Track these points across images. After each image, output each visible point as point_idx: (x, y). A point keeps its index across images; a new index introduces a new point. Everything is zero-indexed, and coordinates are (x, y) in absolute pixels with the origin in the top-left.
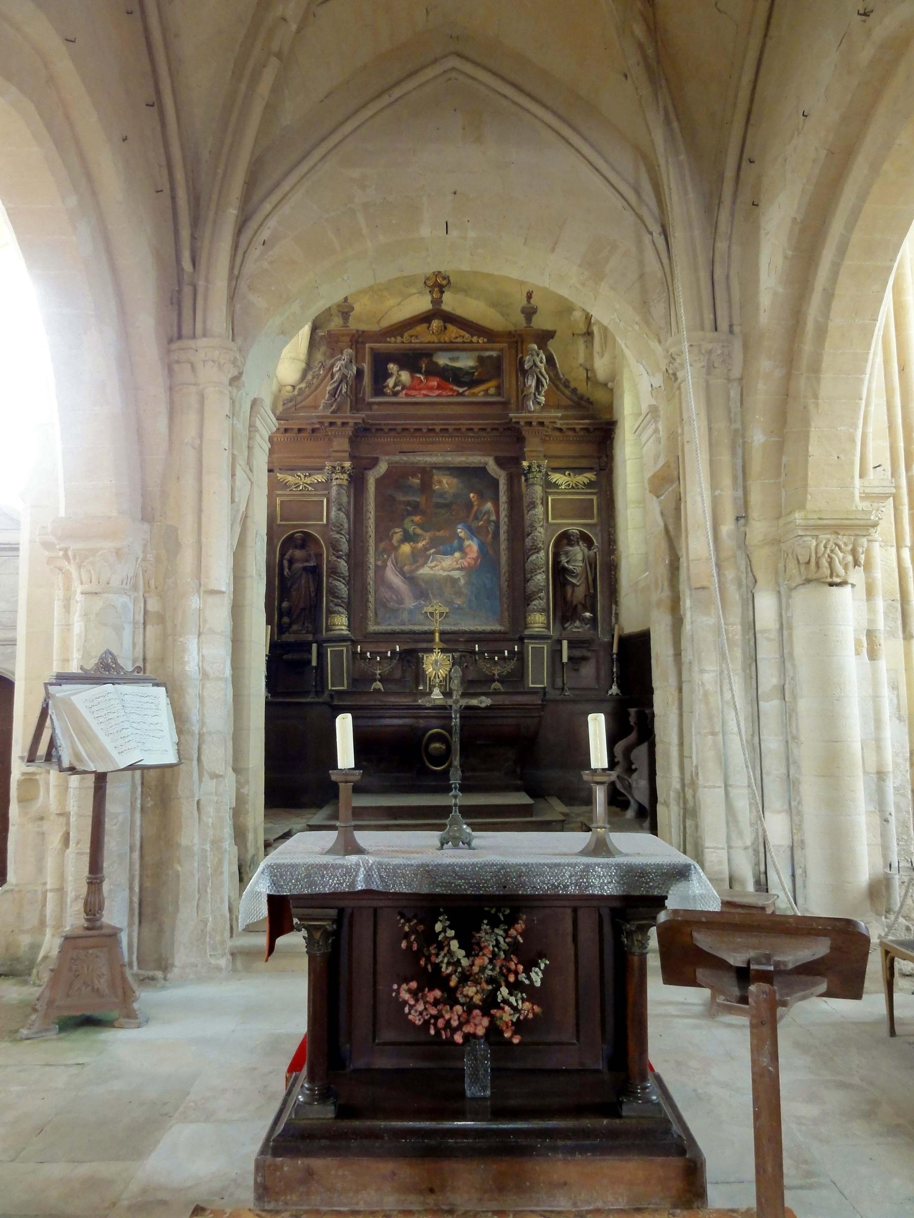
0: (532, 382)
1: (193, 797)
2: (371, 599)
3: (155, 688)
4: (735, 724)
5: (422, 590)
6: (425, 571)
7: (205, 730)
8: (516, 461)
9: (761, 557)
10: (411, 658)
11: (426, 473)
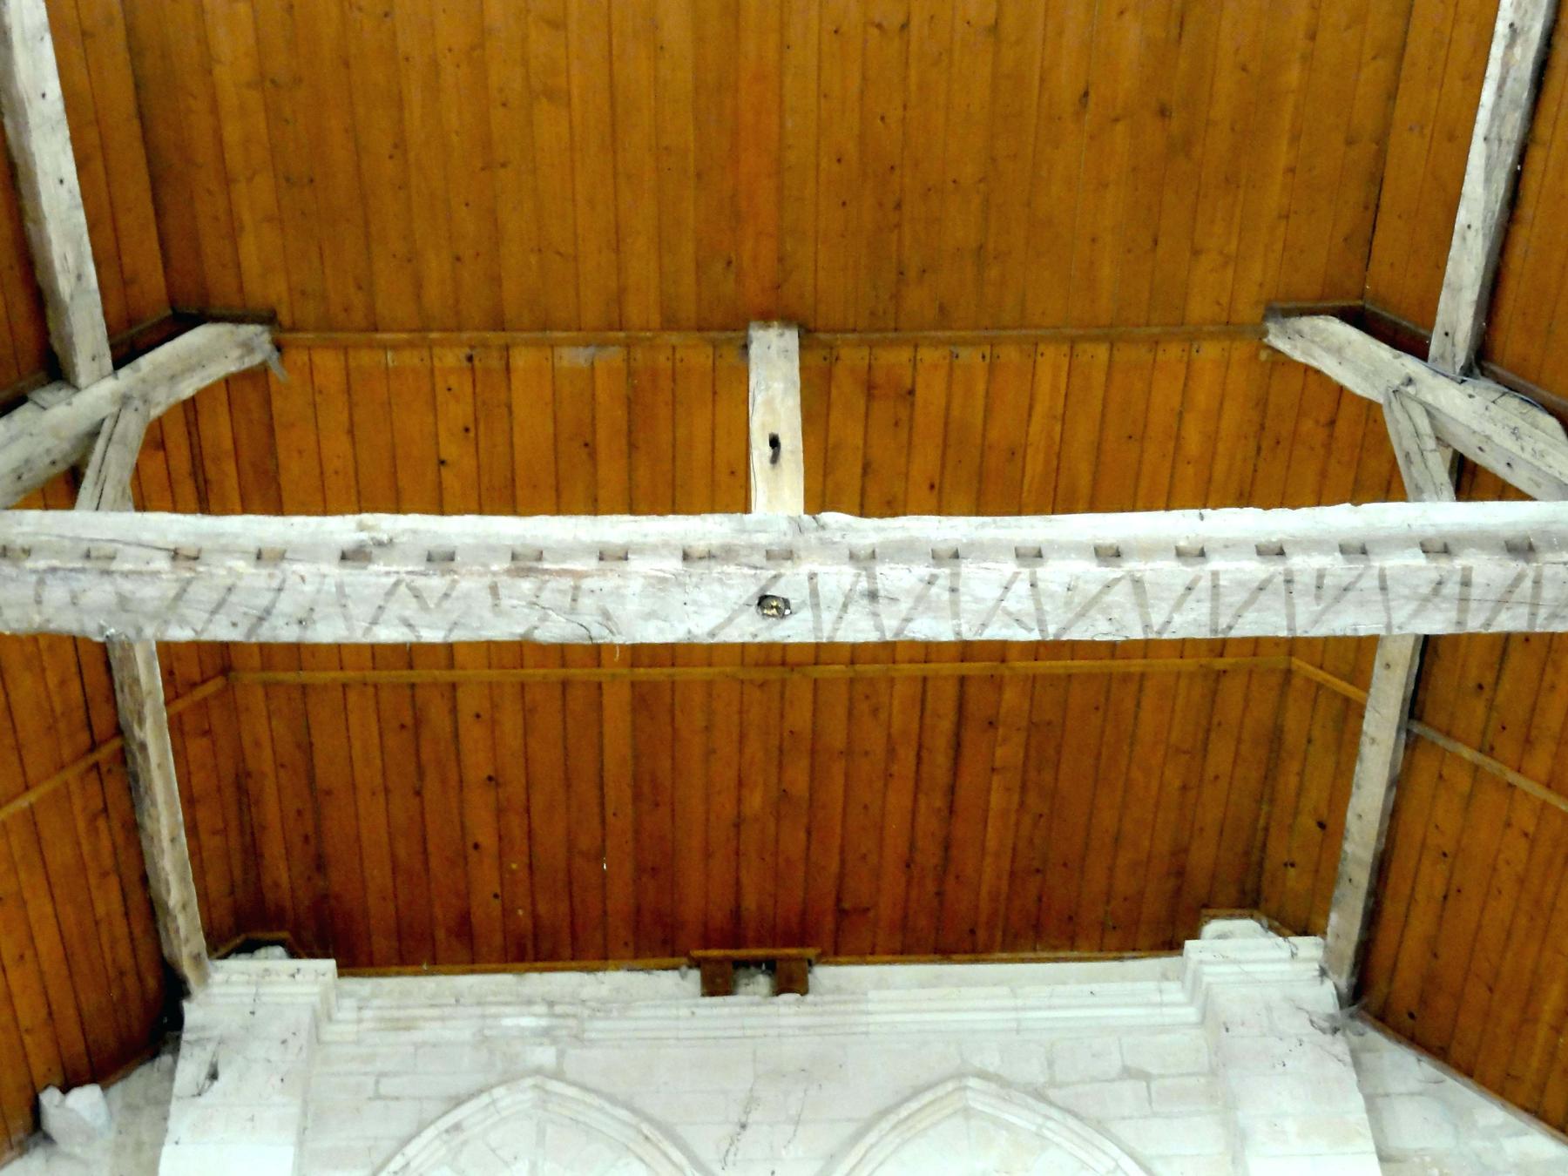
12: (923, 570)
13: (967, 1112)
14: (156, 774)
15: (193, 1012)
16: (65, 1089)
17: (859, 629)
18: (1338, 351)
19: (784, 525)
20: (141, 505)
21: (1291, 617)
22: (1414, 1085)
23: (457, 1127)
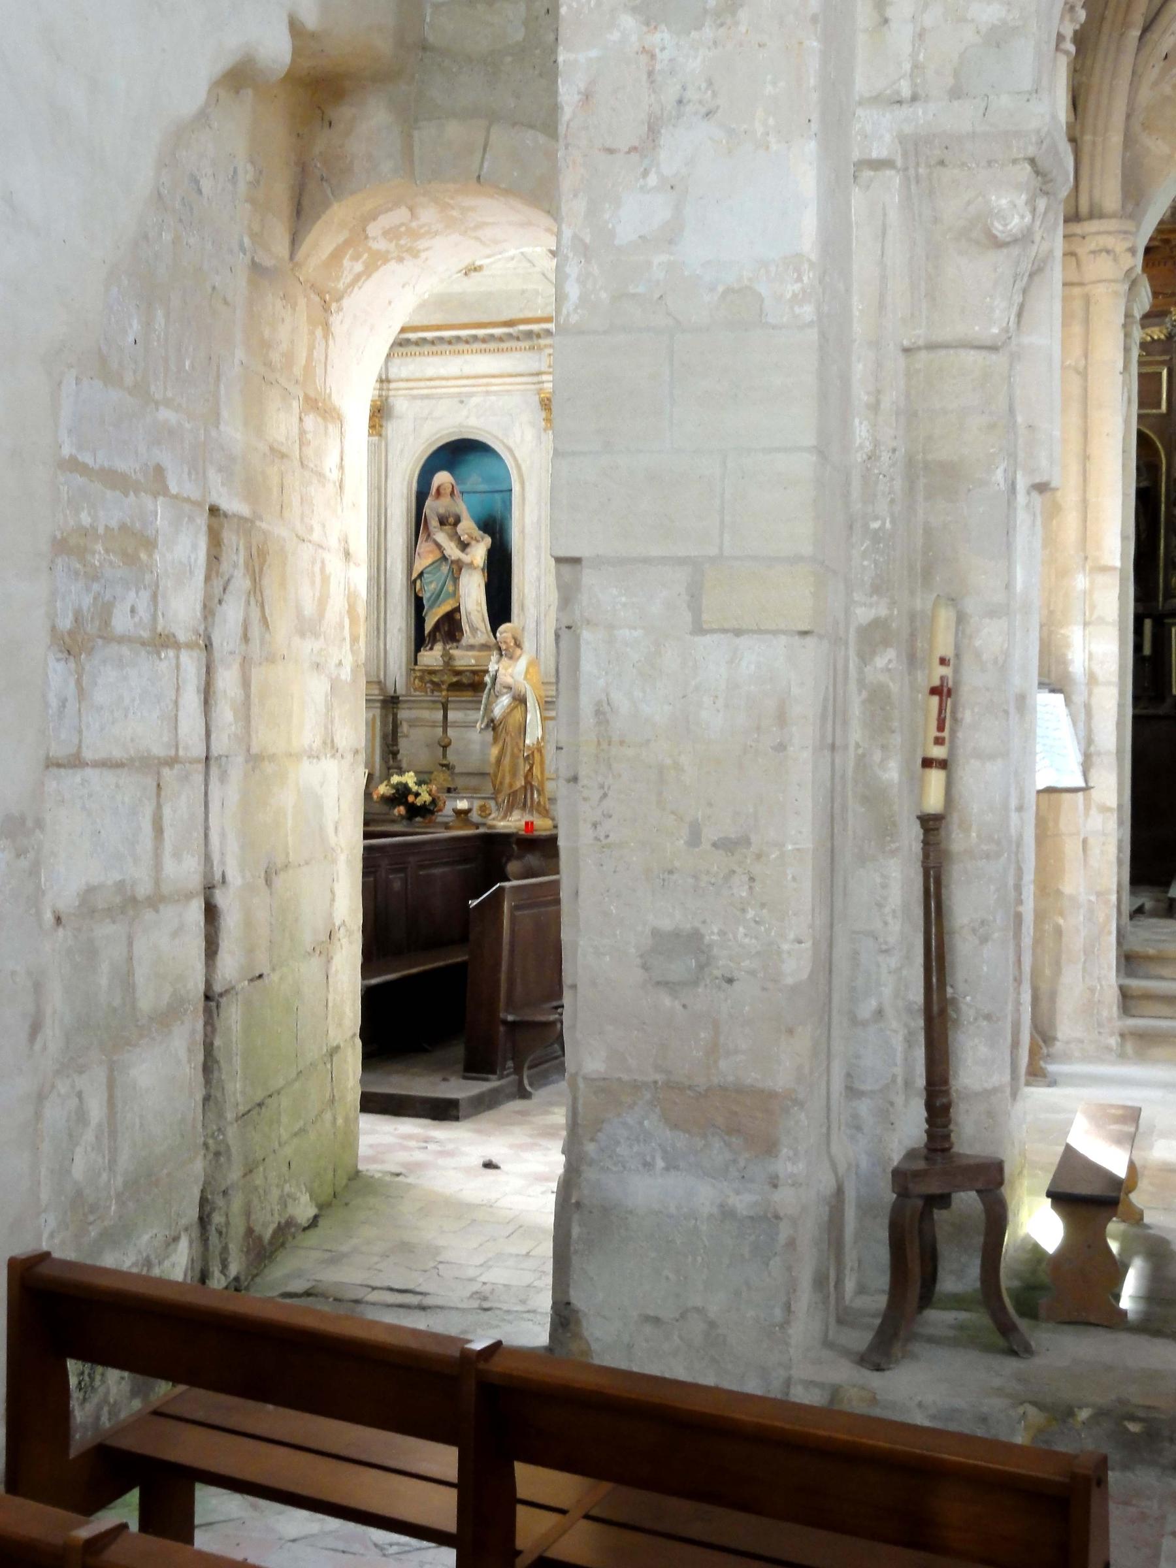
1: (1078, 833)
3: (1053, 695)
7: (1092, 749)
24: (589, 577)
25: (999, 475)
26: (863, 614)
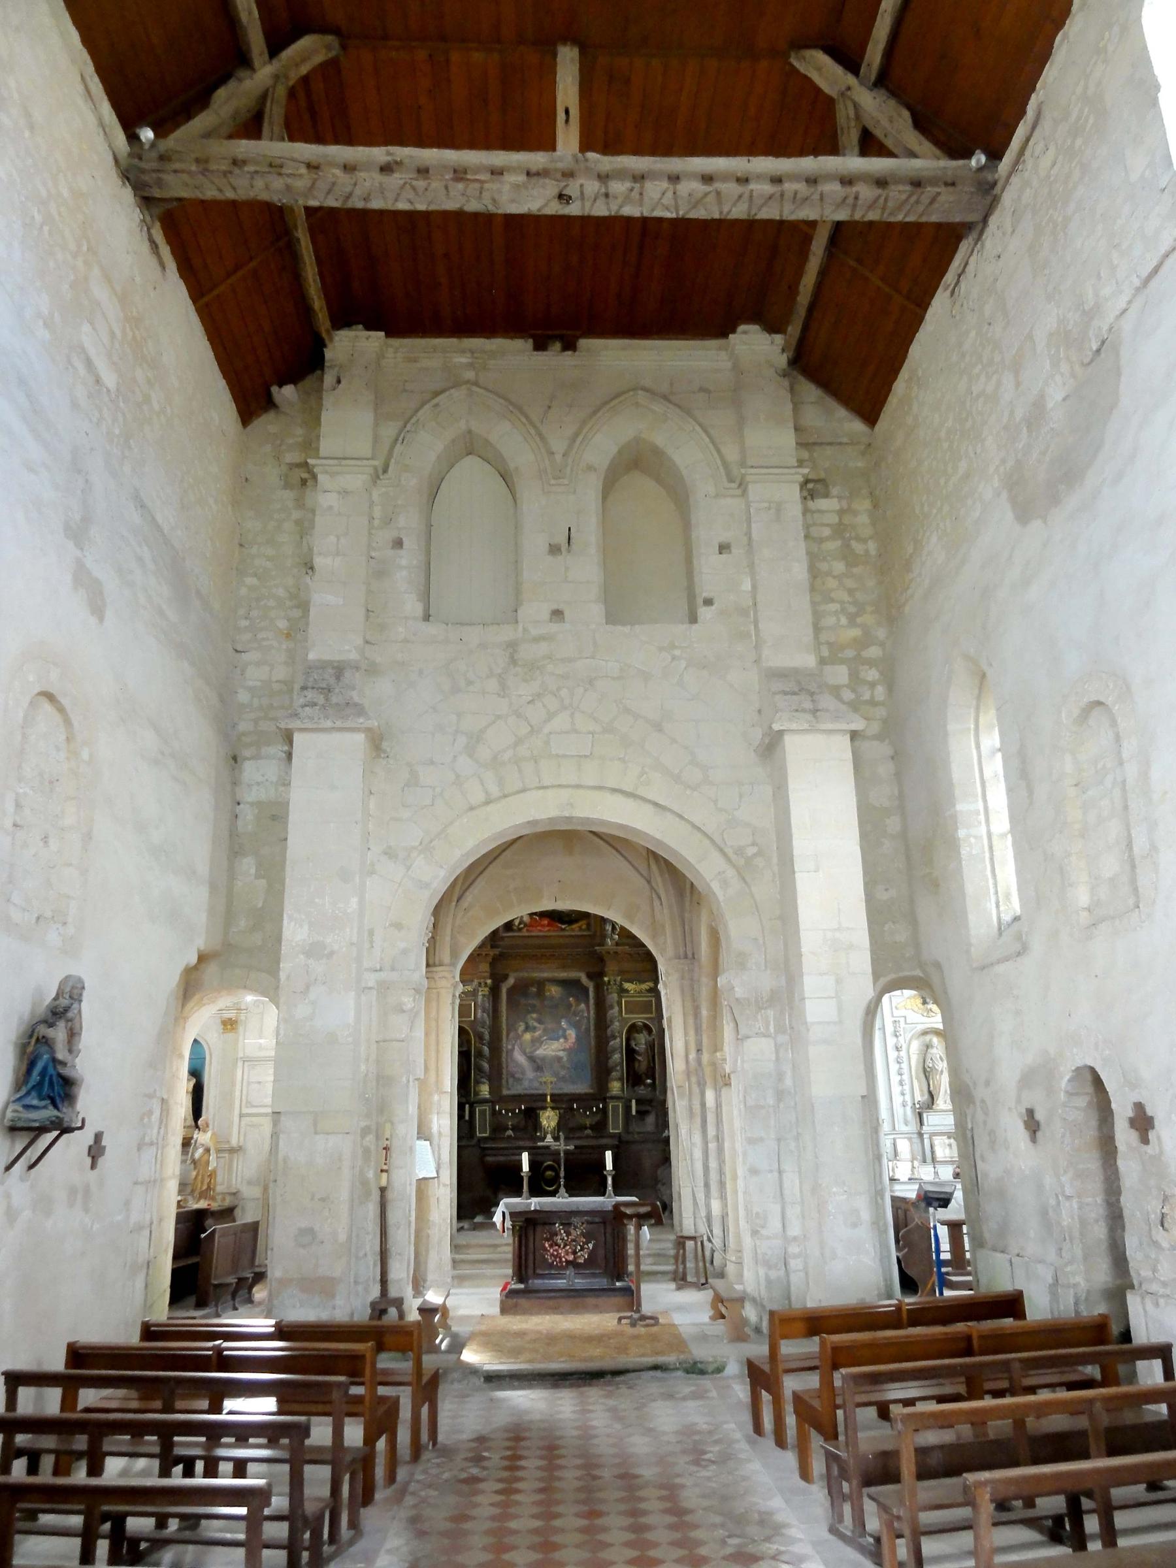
0: (609, 928)
2: (504, 1071)
4: (698, 1154)
5: (538, 1065)
6: (540, 1052)
8: (601, 974)
9: (708, 1071)
10: (531, 1115)
11: (541, 984)
12: (628, 185)
13: (637, 404)
14: (304, 252)
15: (328, 354)
16: (280, 386)
17: (600, 210)
18: (819, 69)
19: (570, 158)
20: (292, 139)
21: (781, 211)
22: (812, 399)
23: (437, 405)
24: (283, 1118)
25: (404, 1079)
26: (363, 1124)
